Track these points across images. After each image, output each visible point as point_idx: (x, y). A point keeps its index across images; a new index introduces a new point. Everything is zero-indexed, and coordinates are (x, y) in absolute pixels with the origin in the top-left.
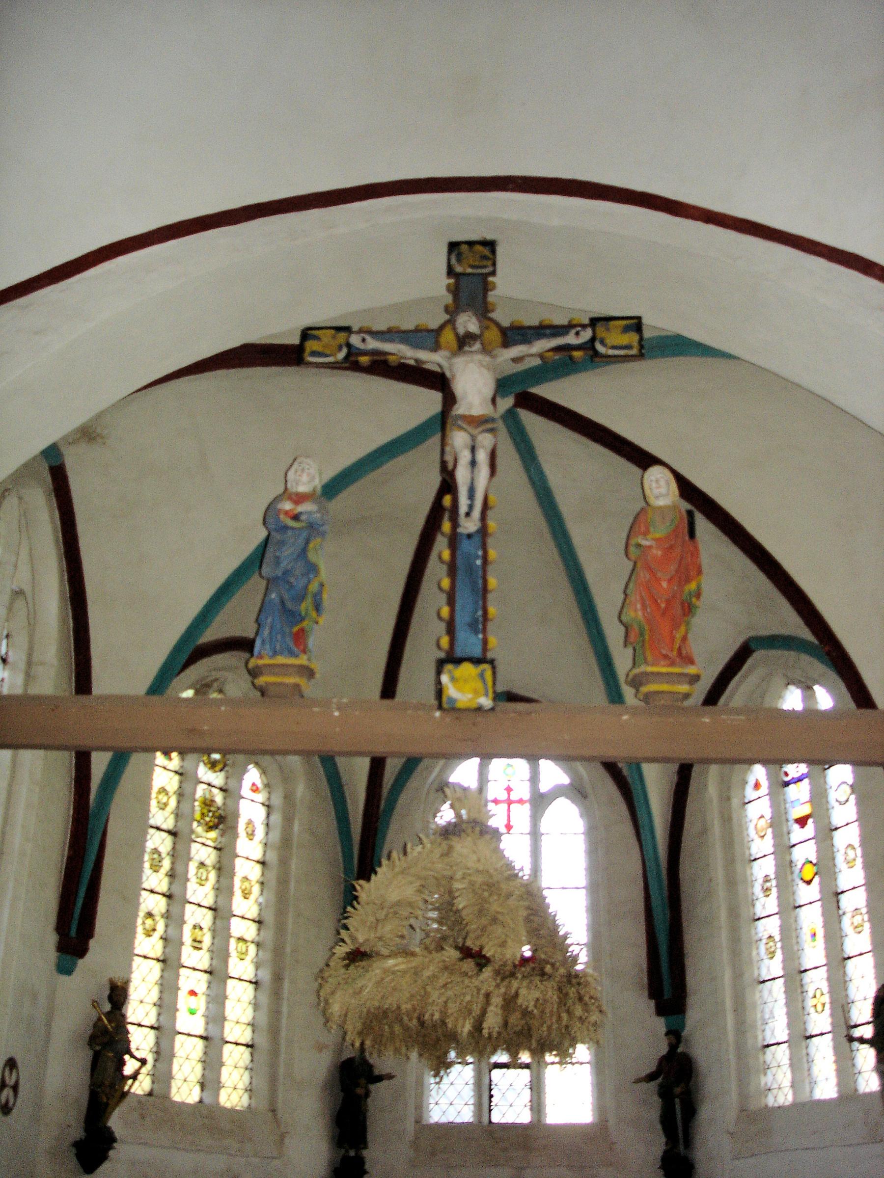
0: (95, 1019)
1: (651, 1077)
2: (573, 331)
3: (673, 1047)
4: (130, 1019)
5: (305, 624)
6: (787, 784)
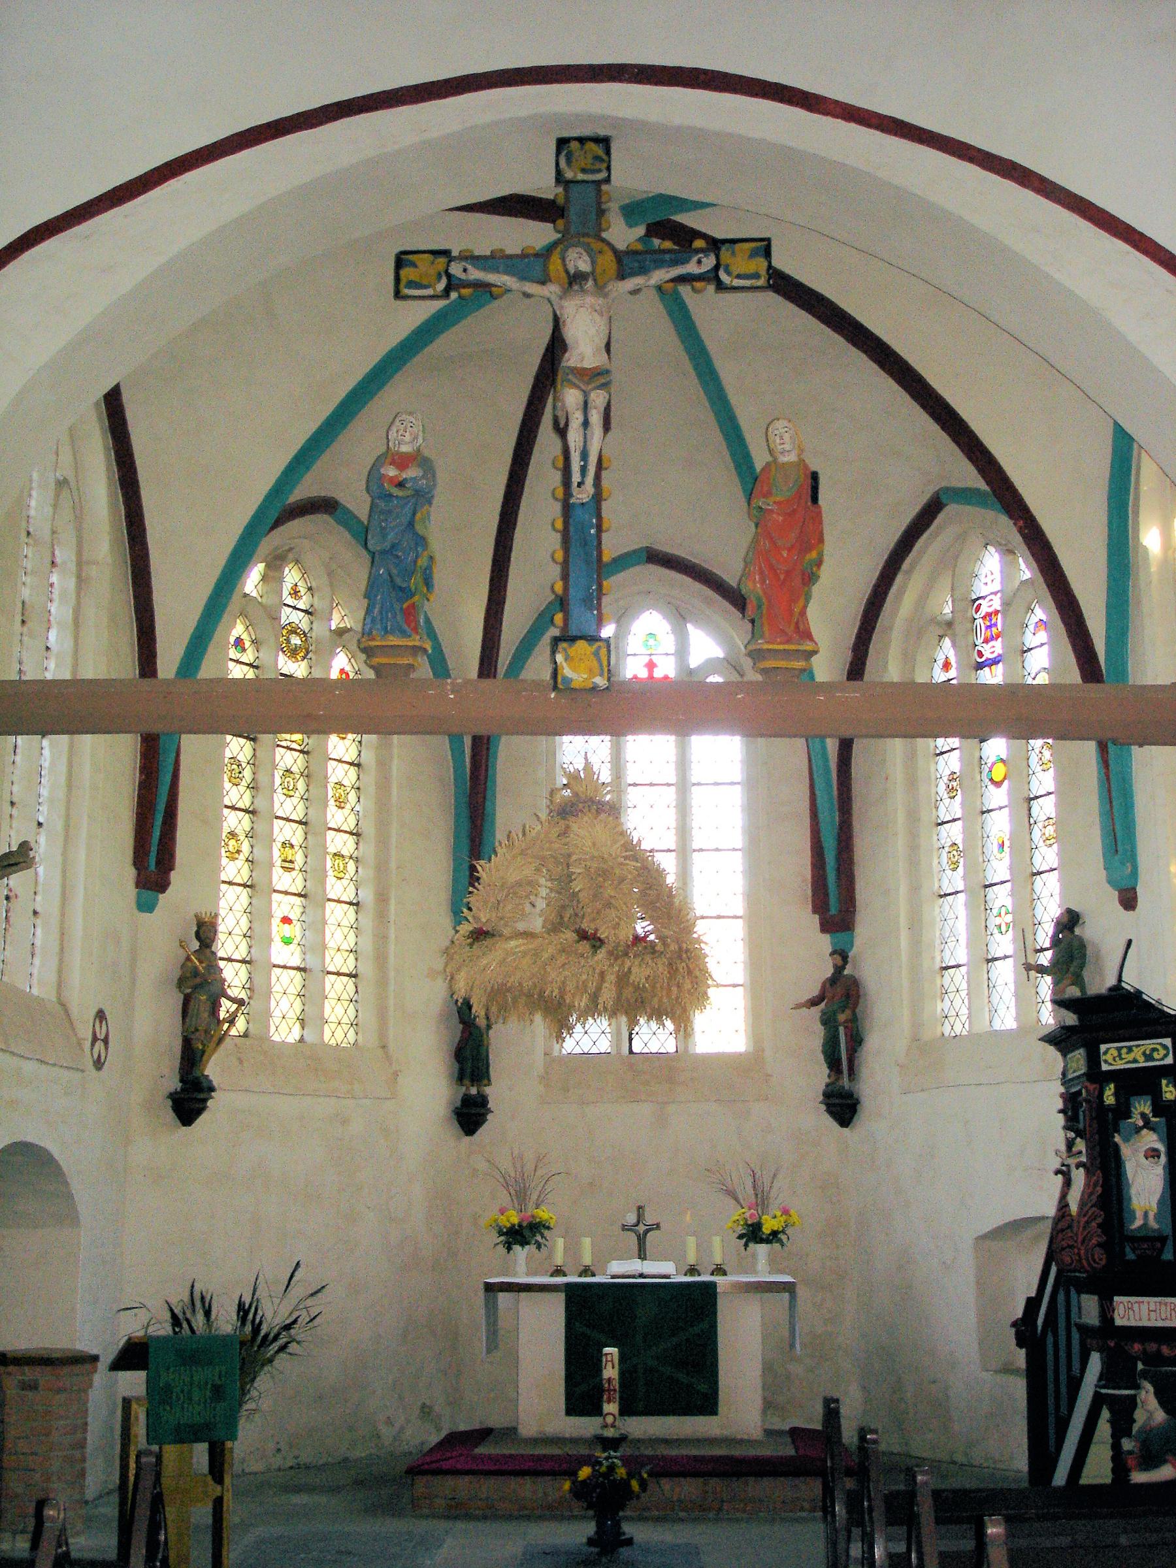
0: (182, 959)
1: (814, 1002)
2: (695, 259)
3: (839, 970)
4: (220, 954)
5: (416, 598)
6: (980, 666)
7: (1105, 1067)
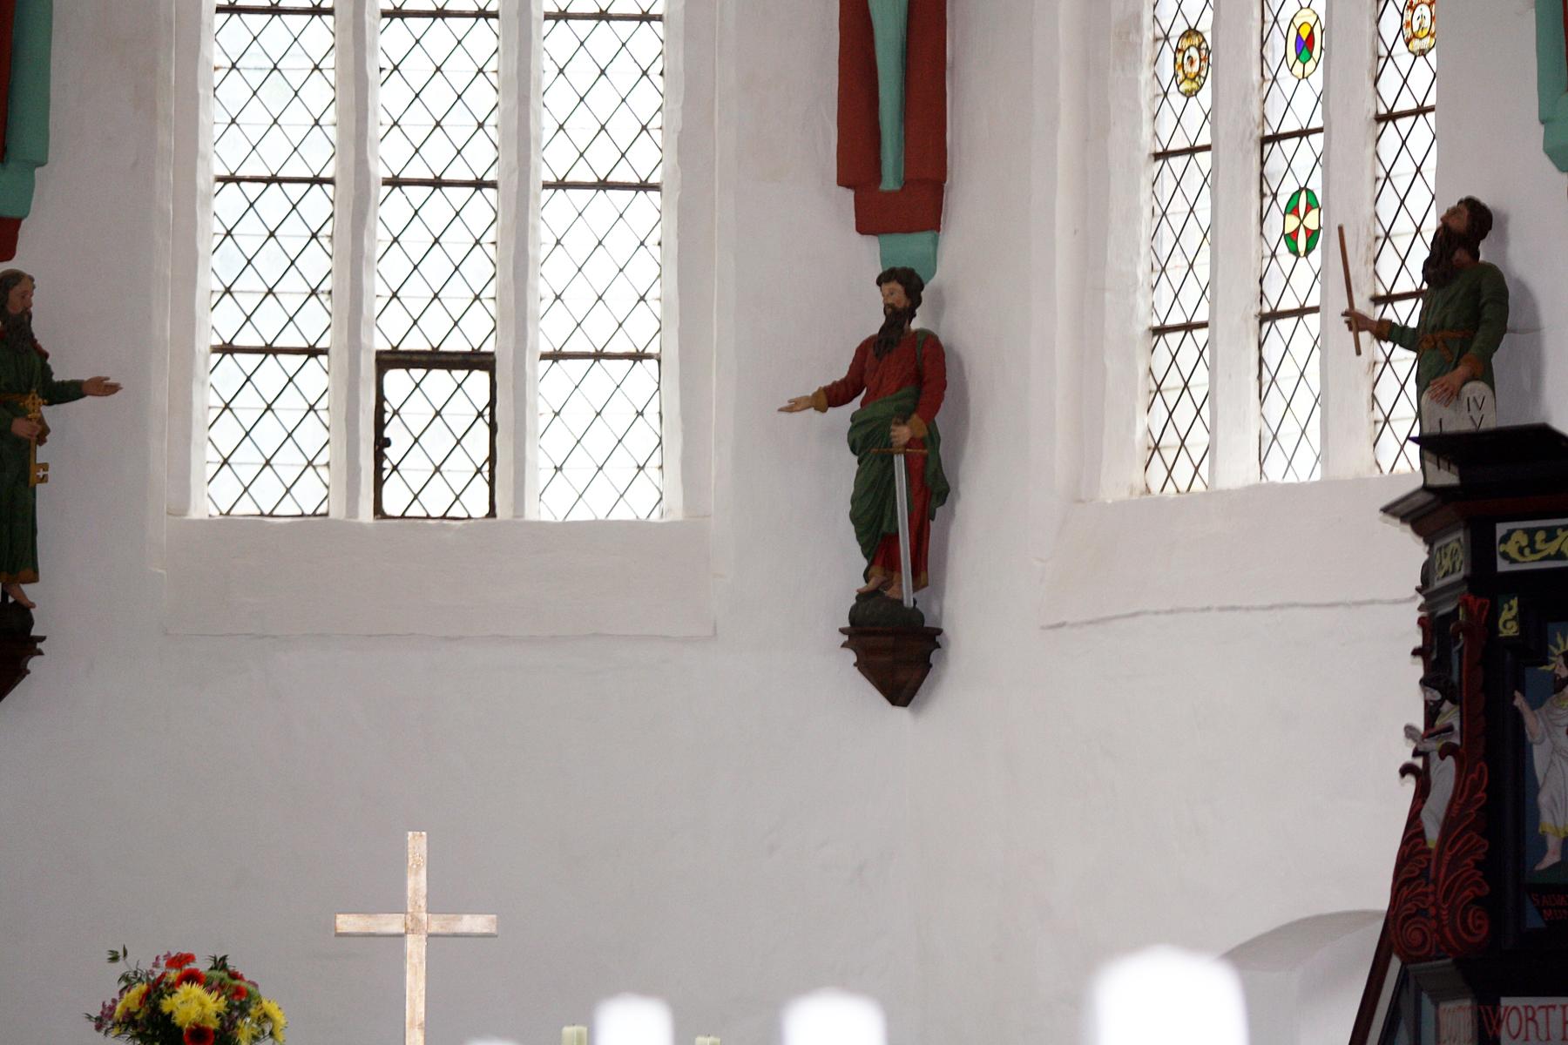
1: (833, 396)
3: (897, 318)
7: (1503, 566)
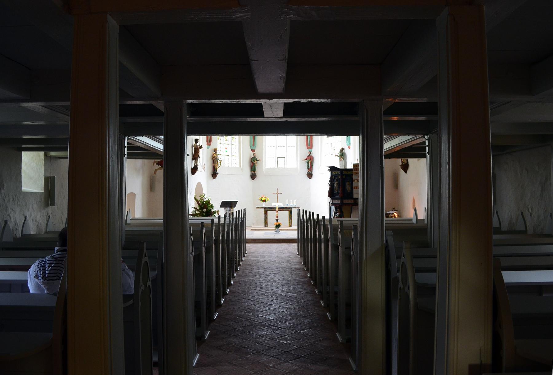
1: (306, 160)
3: (309, 155)
4: (218, 154)
